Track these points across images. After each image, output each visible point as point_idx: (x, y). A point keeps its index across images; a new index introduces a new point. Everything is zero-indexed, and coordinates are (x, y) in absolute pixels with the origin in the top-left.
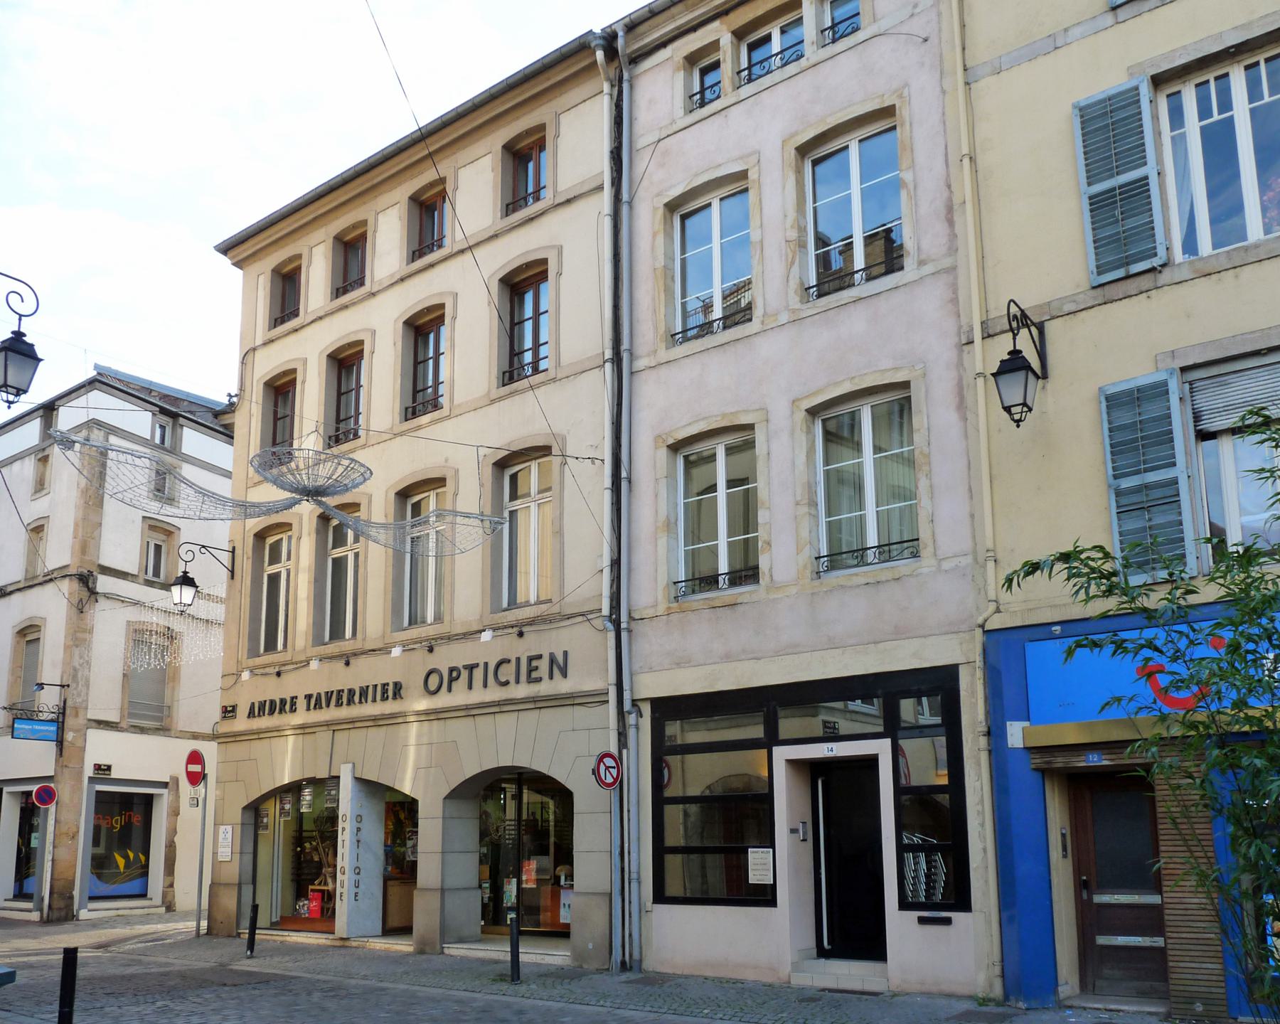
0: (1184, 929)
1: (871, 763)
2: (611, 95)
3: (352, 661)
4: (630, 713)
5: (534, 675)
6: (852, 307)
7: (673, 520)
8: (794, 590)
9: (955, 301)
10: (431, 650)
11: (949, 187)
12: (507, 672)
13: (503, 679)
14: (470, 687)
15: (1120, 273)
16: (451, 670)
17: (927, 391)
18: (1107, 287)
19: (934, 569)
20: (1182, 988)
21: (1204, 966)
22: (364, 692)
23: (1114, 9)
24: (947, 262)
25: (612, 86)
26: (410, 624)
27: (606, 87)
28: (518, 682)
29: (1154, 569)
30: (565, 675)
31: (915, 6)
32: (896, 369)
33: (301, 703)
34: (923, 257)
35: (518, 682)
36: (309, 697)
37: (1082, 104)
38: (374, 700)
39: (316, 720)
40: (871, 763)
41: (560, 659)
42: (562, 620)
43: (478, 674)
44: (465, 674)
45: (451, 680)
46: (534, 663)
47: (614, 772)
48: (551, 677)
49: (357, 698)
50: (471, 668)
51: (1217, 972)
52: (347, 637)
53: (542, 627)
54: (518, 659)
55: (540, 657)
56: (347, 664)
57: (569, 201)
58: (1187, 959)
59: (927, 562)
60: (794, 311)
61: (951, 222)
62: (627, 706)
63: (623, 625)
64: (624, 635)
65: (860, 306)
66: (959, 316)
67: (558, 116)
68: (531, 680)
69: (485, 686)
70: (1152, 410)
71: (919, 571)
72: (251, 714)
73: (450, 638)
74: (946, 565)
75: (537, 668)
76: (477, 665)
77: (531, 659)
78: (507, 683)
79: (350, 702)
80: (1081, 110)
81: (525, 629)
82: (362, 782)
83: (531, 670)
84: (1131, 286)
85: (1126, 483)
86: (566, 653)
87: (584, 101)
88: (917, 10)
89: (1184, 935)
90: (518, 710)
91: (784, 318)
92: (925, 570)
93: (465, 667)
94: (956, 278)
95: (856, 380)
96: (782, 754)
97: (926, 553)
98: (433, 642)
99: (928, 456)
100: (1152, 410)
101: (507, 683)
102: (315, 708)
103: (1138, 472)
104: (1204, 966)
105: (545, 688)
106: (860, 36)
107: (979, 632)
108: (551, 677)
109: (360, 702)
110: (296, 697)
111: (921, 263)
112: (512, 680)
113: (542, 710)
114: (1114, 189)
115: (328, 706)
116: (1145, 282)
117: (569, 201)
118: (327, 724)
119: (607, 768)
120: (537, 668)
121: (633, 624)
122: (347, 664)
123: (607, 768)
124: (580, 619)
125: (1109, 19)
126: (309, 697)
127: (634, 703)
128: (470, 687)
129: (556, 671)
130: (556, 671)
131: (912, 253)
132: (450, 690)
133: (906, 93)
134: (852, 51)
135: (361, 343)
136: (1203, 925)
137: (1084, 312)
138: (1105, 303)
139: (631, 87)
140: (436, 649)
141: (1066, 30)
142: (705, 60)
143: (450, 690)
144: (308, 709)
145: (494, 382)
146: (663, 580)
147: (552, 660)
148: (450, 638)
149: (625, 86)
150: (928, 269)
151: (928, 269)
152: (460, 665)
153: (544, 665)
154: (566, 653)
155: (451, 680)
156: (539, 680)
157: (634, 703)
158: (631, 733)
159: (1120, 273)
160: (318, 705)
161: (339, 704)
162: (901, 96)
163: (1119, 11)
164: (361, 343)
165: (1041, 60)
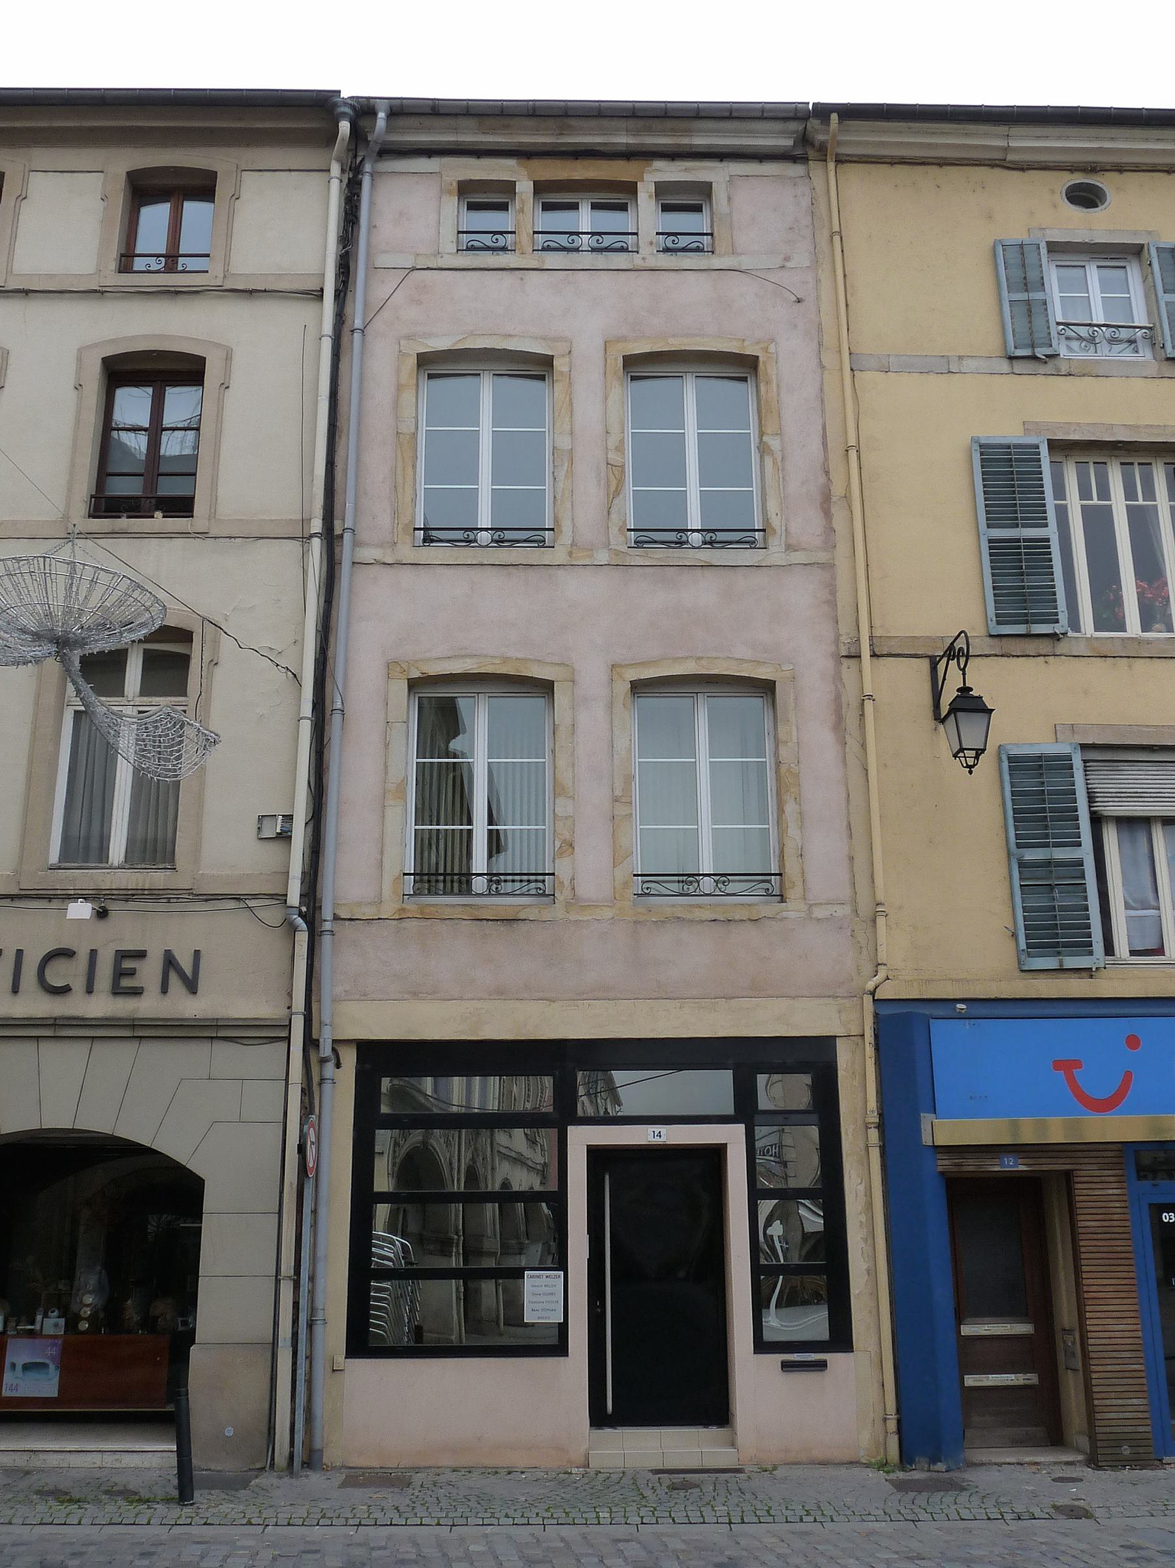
0: (1108, 1361)
1: (717, 1153)
2: (341, 181)
5: (126, 982)
6: (699, 571)
8: (608, 913)
9: (832, 603)
11: (827, 473)
13: (58, 983)
15: (1020, 629)
17: (796, 699)
18: (1005, 640)
19: (803, 915)
20: (1108, 1430)
21: (1129, 1402)
23: (1011, 358)
24: (822, 557)
25: (343, 171)
27: (335, 169)
28: (90, 990)
29: (1059, 953)
30: (192, 986)
31: (787, 259)
32: (759, 663)
34: (791, 541)
35: (90, 990)
37: (983, 442)
40: (717, 1153)
41: (186, 965)
42: (192, 901)
46: (127, 964)
48: (164, 990)
51: (1142, 1408)
53: (150, 906)
54: (93, 953)
55: (141, 955)
57: (250, 293)
58: (1113, 1395)
59: (794, 909)
60: (617, 553)
61: (827, 514)
65: (708, 573)
66: (837, 623)
68: (117, 991)
70: (1053, 783)
71: (785, 914)
74: (819, 913)
75: (132, 973)
77: (122, 955)
78: (65, 990)
80: (981, 446)
81: (111, 906)
83: (120, 973)
84: (1031, 646)
85: (1031, 855)
87: (290, 170)
88: (788, 264)
89: (1109, 1368)
90: (93, 1038)
91: (602, 557)
92: (792, 915)
94: (834, 578)
95: (704, 662)
96: (580, 1138)
97: (793, 894)
99: (797, 776)
100: (1053, 783)
101: (65, 990)
103: (1046, 845)
104: (1129, 1402)
105: (149, 1006)
106: (716, 262)
107: (868, 1000)
108: (164, 990)
111: (789, 548)
112: (78, 985)
113: (144, 1041)
114: (1018, 540)
116: (1044, 646)
117: (250, 293)
120: (132, 973)
121: (337, 927)
124: (232, 904)
125: (1005, 366)
129: (173, 978)
131: (778, 532)
133: (772, 348)
134: (704, 274)
136: (1128, 1355)
137: (979, 658)
138: (1002, 656)
141: (960, 358)
147: (170, 962)
150: (798, 557)
151: (798, 557)
156: (137, 992)
159: (1020, 629)
162: (766, 350)
163: (1015, 362)
165: (932, 377)
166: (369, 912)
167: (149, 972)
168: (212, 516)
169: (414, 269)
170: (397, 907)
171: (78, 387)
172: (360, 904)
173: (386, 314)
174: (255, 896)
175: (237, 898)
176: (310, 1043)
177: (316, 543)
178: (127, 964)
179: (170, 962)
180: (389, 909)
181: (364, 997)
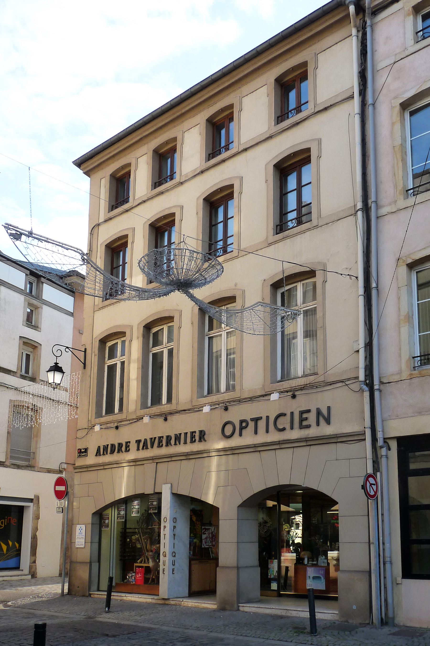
2: (358, 36)
3: (169, 418)
4: (381, 447)
5: (305, 423)
7: (411, 315)
10: (226, 409)
12: (284, 422)
13: (281, 427)
14: (256, 432)
16: (242, 422)
22: (178, 438)
25: (358, 31)
26: (209, 393)
27: (354, 31)
28: (292, 428)
30: (328, 421)
33: (133, 446)
35: (292, 428)
36: (138, 442)
38: (185, 443)
39: (143, 457)
41: (325, 412)
42: (325, 386)
43: (262, 424)
44: (252, 425)
45: (242, 429)
46: (305, 416)
47: (375, 487)
48: (318, 424)
49: (173, 442)
50: (256, 420)
52: (163, 403)
53: (310, 391)
54: (292, 413)
55: (309, 411)
56: (166, 420)
57: (326, 109)
62: (380, 442)
63: (376, 387)
64: (377, 394)
67: (316, 55)
68: (301, 427)
69: (267, 431)
72: (98, 453)
73: (240, 401)
75: (306, 419)
76: (261, 418)
77: (302, 413)
78: (284, 429)
79: (168, 443)
81: (296, 393)
82: (177, 496)
83: (302, 420)
86: (329, 408)
87: (337, 43)
90: (294, 447)
93: (252, 420)
98: (228, 404)
101: (284, 429)
102: (143, 449)
105: (313, 432)
108: (318, 424)
109: (175, 444)
110: (130, 442)
112: (288, 426)
113: (311, 447)
115: (152, 447)
117: (326, 109)
118: (152, 459)
119: (371, 485)
120: (306, 419)
121: (382, 387)
122: (166, 420)
123: (371, 485)
124: (340, 384)
126: (138, 442)
127: (385, 440)
128: (256, 432)
129: (321, 419)
130: (321, 420)
132: (241, 435)
135: (308, 150)
139: (372, 31)
140: (230, 408)
142: (424, 10)
143: (241, 435)
144: (138, 449)
145: (271, 232)
146: (405, 356)
147: (319, 413)
148: (240, 401)
149: (368, 30)
152: (248, 419)
153: (312, 417)
154: (329, 408)
155: (242, 429)
156: (308, 427)
157: (385, 440)
158: (383, 461)
160: (145, 446)
161: (160, 446)
164: (308, 150)
166: (396, 378)
167: (312, 417)
168: (319, 216)
169: (395, 63)
170: (408, 373)
171: (266, 181)
172: (392, 375)
173: (384, 91)
174: (349, 379)
175: (342, 381)
176: (374, 439)
177: (360, 214)
178: (305, 416)
179: (319, 413)
180: (405, 375)
181: (398, 417)
